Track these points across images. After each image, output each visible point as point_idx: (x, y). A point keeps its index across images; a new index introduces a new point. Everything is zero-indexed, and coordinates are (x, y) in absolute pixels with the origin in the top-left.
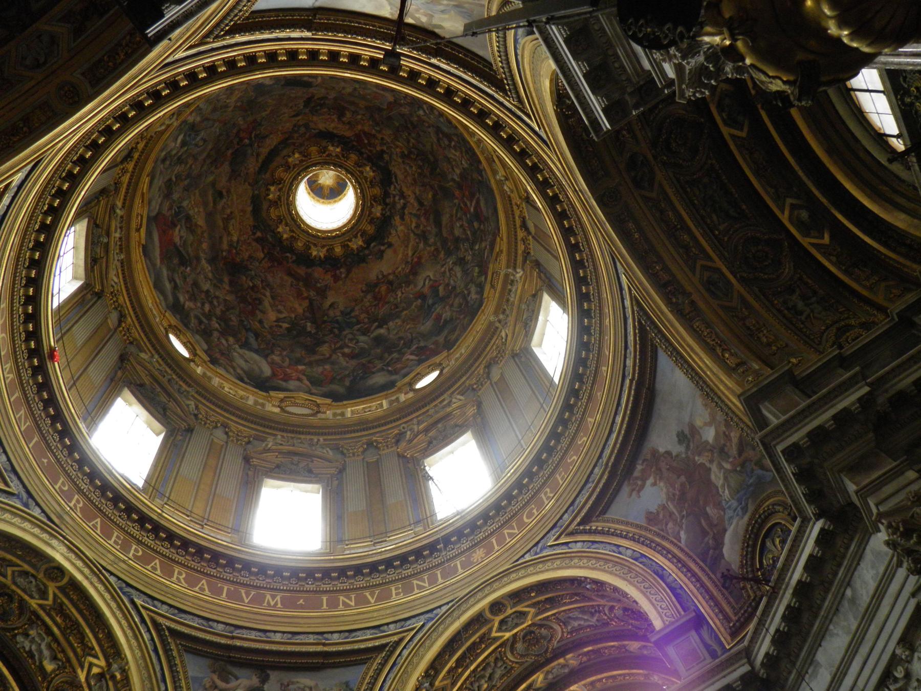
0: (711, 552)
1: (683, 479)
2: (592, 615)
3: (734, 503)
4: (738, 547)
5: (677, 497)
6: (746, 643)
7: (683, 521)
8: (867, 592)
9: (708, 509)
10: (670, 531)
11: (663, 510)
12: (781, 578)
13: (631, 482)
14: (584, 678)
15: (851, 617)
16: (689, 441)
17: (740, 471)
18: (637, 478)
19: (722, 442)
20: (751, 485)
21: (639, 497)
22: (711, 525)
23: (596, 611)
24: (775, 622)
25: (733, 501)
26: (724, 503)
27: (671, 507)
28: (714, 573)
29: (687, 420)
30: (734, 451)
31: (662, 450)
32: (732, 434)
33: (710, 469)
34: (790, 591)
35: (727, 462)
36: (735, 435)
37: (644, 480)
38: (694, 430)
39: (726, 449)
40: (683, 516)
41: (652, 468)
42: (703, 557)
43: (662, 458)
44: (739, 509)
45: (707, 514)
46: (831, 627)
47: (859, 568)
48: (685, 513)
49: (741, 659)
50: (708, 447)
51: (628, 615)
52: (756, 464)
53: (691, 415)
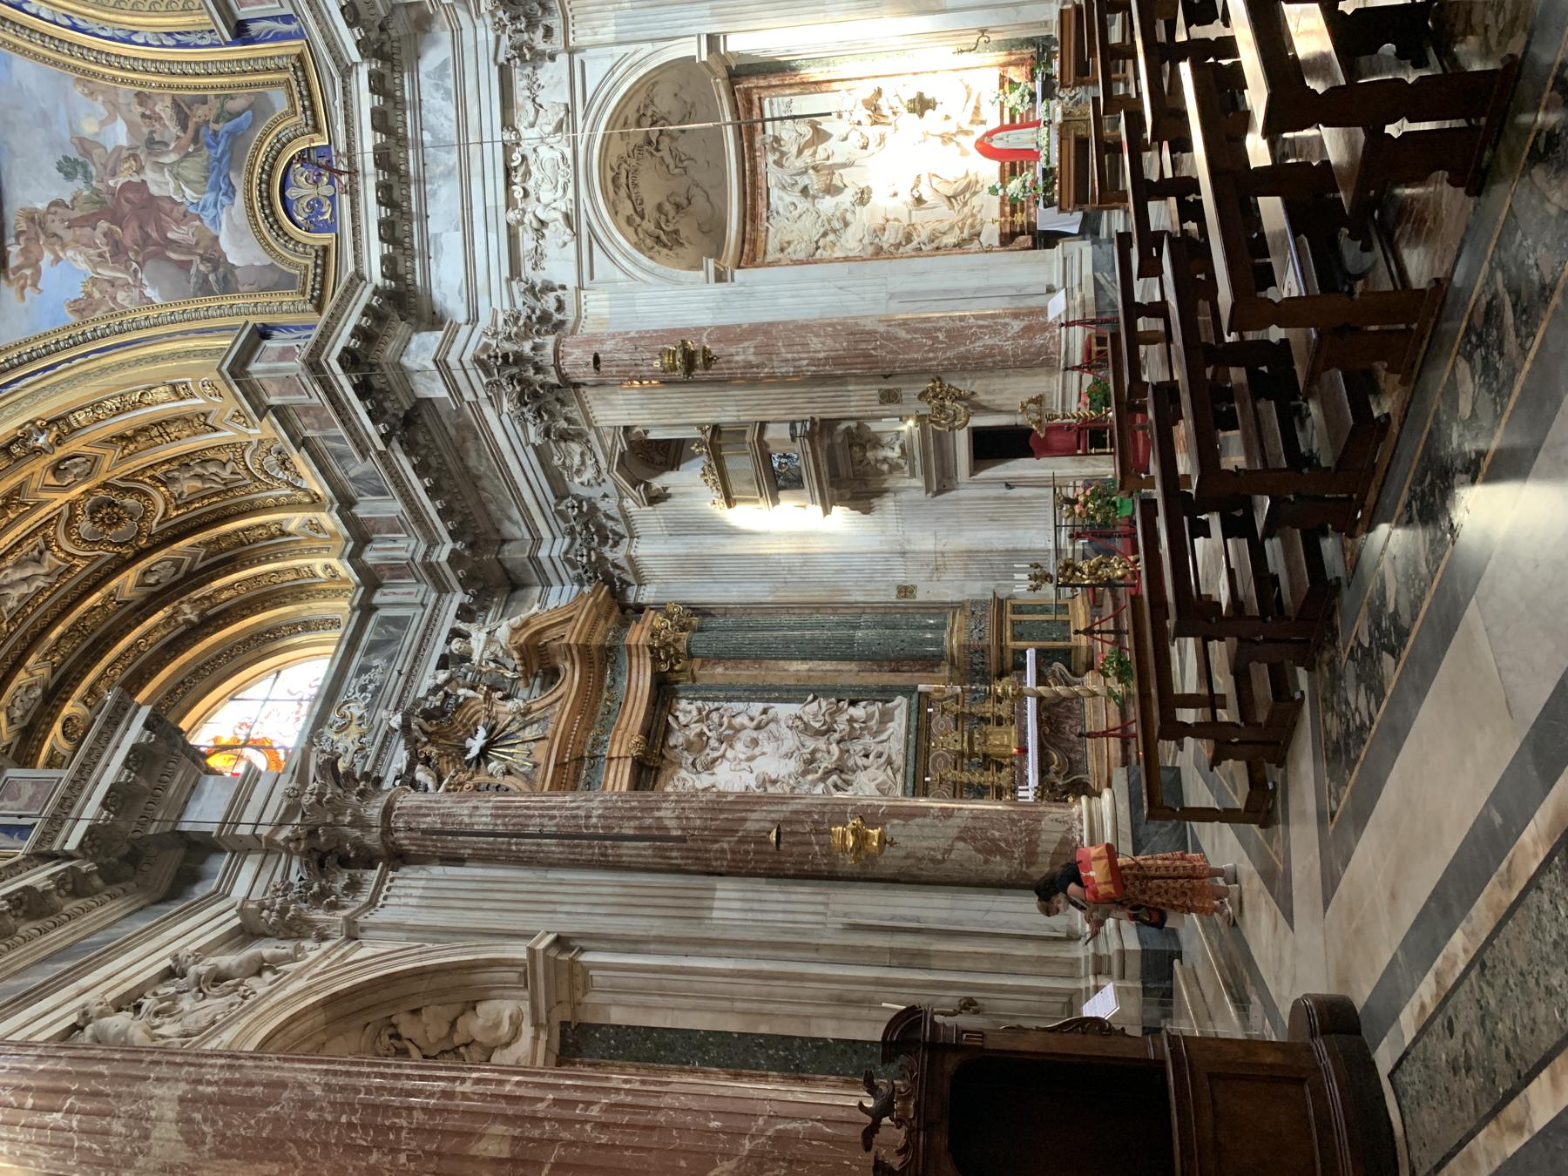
0: (211, 278)
1: (103, 225)
2: (38, 561)
3: (210, 197)
4: (251, 239)
5: (108, 255)
6: (351, 268)
7: (140, 275)
8: (446, 117)
9: (170, 235)
10: (126, 303)
11: (94, 285)
12: (351, 163)
13: (11, 277)
14: (74, 687)
15: (442, 155)
16: (84, 166)
17: (195, 151)
18: (19, 268)
19: (146, 130)
20: (223, 154)
21: (40, 291)
22: (189, 249)
23: (41, 553)
24: (372, 212)
25: (206, 196)
26: (192, 210)
27: (106, 273)
28: (237, 291)
29: (67, 136)
30: (174, 129)
31: (41, 206)
32: (157, 109)
33: (144, 182)
34: (370, 166)
35: (167, 153)
36: (164, 109)
37: (35, 265)
38: (85, 145)
39: (157, 137)
40: (135, 271)
41: (38, 240)
42: (205, 289)
43: (49, 217)
44: (220, 197)
45: (172, 241)
46: (428, 187)
47: (424, 104)
48: (135, 265)
49: (357, 286)
50: (125, 154)
51: (102, 519)
52: (216, 122)
53: (70, 124)
